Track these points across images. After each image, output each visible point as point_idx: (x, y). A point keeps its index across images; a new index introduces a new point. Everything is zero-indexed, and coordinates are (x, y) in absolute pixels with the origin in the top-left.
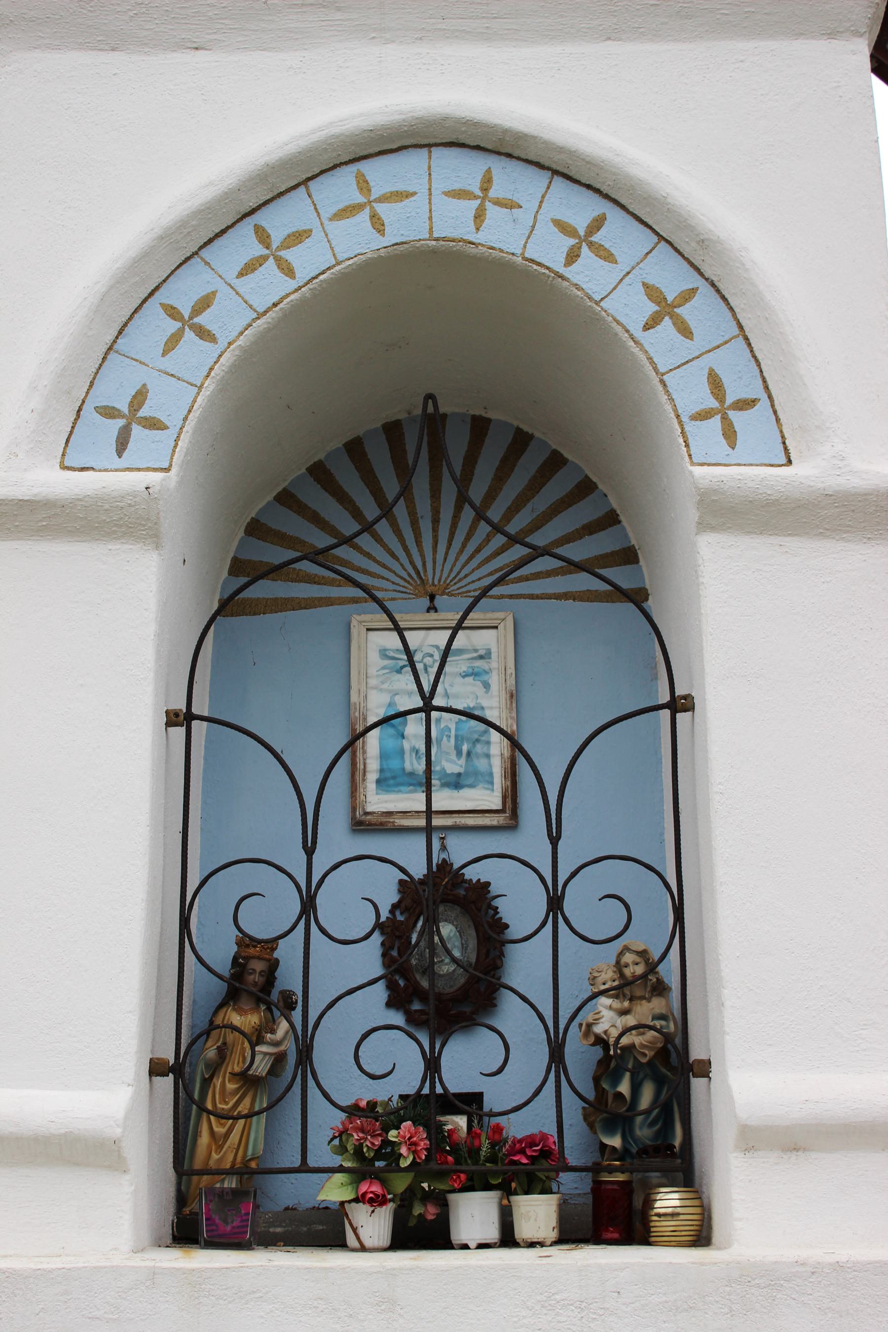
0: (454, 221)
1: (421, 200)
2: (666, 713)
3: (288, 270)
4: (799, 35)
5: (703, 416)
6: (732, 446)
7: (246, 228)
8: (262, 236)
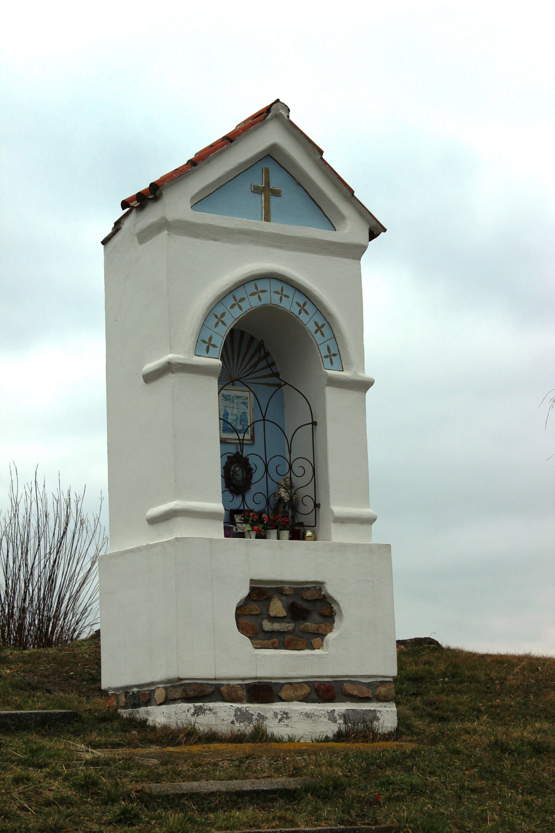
0: (276, 299)
1: (268, 293)
2: (311, 425)
3: (241, 308)
4: (347, 257)
5: (326, 357)
6: (332, 365)
7: (231, 296)
8: (235, 298)
